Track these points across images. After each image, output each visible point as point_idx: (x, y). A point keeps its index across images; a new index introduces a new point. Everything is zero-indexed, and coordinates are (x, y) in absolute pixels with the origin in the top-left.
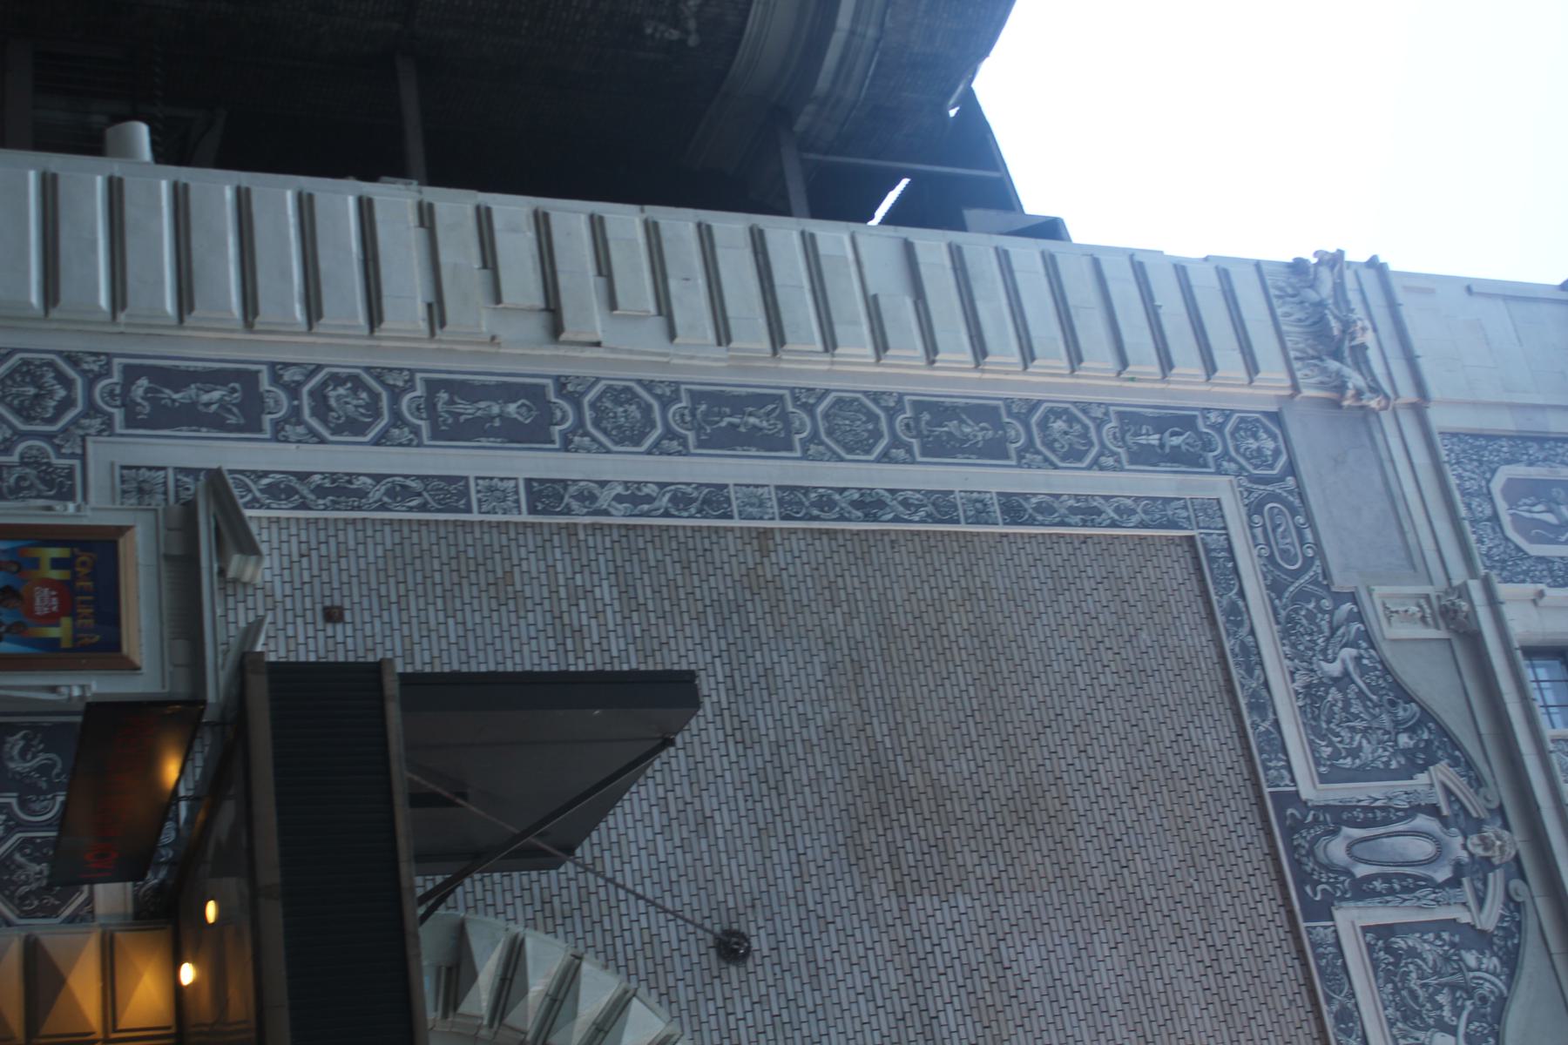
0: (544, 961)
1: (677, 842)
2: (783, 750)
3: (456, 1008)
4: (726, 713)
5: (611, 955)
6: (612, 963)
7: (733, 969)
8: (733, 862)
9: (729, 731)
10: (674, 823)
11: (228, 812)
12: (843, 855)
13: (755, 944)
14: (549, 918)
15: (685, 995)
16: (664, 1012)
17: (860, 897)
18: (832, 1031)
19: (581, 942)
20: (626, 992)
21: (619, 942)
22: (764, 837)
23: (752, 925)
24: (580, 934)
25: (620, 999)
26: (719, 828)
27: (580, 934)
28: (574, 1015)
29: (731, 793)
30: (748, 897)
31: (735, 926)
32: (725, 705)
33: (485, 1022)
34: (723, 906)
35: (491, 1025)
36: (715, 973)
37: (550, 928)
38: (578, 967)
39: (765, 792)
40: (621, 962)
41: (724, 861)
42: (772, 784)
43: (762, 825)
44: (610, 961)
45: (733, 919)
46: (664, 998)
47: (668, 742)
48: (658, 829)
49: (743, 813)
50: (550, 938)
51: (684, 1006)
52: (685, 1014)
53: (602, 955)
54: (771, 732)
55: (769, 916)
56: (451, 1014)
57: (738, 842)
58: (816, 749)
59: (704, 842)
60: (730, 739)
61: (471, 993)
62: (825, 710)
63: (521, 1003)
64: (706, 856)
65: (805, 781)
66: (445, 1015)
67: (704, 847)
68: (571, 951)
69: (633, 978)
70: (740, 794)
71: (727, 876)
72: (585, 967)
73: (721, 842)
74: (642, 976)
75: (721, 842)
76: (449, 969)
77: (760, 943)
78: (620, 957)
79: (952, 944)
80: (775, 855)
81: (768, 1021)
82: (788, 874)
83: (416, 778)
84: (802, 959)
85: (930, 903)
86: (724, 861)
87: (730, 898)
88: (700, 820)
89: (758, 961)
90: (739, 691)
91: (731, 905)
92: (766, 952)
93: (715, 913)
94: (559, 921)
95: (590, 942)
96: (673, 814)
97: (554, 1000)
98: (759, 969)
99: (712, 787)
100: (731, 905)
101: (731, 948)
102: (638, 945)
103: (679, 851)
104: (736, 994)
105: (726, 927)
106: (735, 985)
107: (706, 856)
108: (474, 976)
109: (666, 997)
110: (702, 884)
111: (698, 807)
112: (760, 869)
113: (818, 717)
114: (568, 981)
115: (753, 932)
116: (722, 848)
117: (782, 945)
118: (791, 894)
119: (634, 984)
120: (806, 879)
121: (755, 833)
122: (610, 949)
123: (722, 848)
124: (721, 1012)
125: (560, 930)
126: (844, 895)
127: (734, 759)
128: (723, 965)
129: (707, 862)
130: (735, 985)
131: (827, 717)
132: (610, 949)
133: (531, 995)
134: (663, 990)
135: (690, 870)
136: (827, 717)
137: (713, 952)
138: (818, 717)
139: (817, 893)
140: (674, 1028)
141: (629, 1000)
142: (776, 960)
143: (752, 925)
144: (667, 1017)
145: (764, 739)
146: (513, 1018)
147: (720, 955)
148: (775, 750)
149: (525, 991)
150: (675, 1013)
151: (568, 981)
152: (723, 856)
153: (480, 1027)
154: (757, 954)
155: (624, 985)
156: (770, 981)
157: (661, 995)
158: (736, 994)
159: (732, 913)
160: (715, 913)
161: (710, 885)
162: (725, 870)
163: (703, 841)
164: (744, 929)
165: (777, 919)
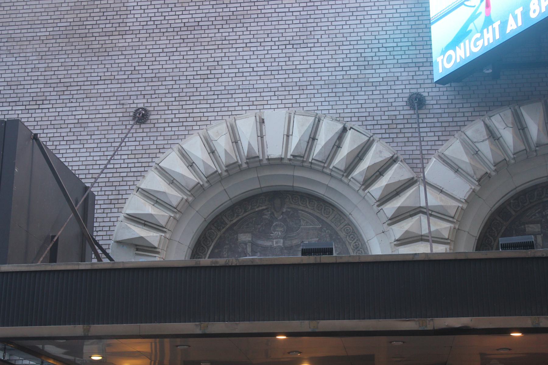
0: (137, 205)
1: (89, 137)
2: (49, 81)
3: (155, 248)
4: (28, 107)
5: (139, 174)
6: (143, 174)
7: (151, 117)
8: (101, 111)
9: (37, 107)
10: (79, 138)
11: (50, 348)
12: (103, 58)
13: (141, 106)
14: (118, 201)
15: (160, 142)
16: (168, 152)
17: (124, 53)
18: (185, 73)
19: (131, 187)
20: (156, 168)
21: (133, 170)
22: (90, 95)
23: (132, 106)
24: (127, 188)
25: (159, 172)
26: (84, 117)
27: (127, 188)
28: (164, 193)
29: (67, 109)
30: (118, 106)
31: (132, 114)
32: (23, 107)
33: (163, 234)
34: (122, 119)
35: (165, 232)
36: (152, 126)
37: (123, 201)
38: (142, 189)
39: (68, 93)
40: (142, 169)
41: (100, 116)
42: (65, 89)
43: (84, 96)
44: (141, 175)
45: (128, 114)
46: (162, 151)
47: (35, 137)
48: (81, 146)
49: (77, 104)
50: (127, 201)
51: (166, 142)
52: (170, 142)
53: (139, 178)
54: (39, 86)
55: (128, 98)
56: (158, 250)
57: (92, 108)
58: (50, 65)
59: (90, 125)
60: (41, 107)
61: (148, 239)
62: (31, 58)
63: (157, 217)
64: (97, 124)
65: (65, 72)
66: (158, 253)
67: (92, 125)
68: (135, 192)
69: (151, 164)
70: (68, 105)
71: (107, 115)
72: (142, 186)
73: (91, 116)
74: (150, 160)
75: (91, 116)
76: (137, 250)
77: (141, 103)
78: (140, 169)
79: (151, 11)
80: (100, 91)
81: (177, 103)
82: (110, 86)
83: (41, 259)
84: (150, 84)
85: (130, 20)
86: (100, 116)
87: (118, 115)
88: (79, 125)
89: (149, 105)
90: (17, 99)
91: (121, 115)
92: (145, 101)
93: (124, 123)
94: (120, 197)
95: (132, 183)
96: (75, 138)
97: (157, 202)
98: (153, 105)
99: (64, 118)
100: (121, 115)
101: (141, 117)
102: (136, 161)
103: (93, 137)
104: (163, 117)
105: (131, 118)
106: (159, 117)
107: (97, 124)
108: (141, 238)
109: (161, 150)
110: (110, 128)
111: (72, 126)
112: (106, 99)
113: (34, 62)
114: (148, 195)
115: (135, 106)
116: (93, 116)
117: (143, 93)
118: (119, 86)
119: (153, 164)
120: (112, 77)
121: (88, 100)
122: (136, 174)
123: (93, 116)
124: (171, 125)
125: (124, 197)
126: (122, 60)
127: (50, 106)
128: (149, 121)
129: (99, 124)
130: (159, 117)
131: (35, 58)
132: (136, 174)
133: (153, 213)
134: (157, 151)
135: (103, 132)
136: (35, 58)
137: (143, 126)
138: (34, 62)
139: (120, 73)
140: (175, 147)
141: (160, 167)
142: (149, 97)
143: (132, 106)
144: (170, 150)
145: (43, 90)
146: (163, 223)
147: (144, 123)
148: (48, 85)
149: (151, 215)
150: (168, 146)
151: (148, 195)
152: (98, 116)
153: (165, 237)
154: (146, 105)
155: (153, 169)
156: (159, 100)
157: (160, 152)
158: (163, 117)
159: (125, 114)
160: (124, 123)
161: (111, 124)
162: (104, 116)
163: (90, 125)
164: (133, 110)
165: (130, 93)
